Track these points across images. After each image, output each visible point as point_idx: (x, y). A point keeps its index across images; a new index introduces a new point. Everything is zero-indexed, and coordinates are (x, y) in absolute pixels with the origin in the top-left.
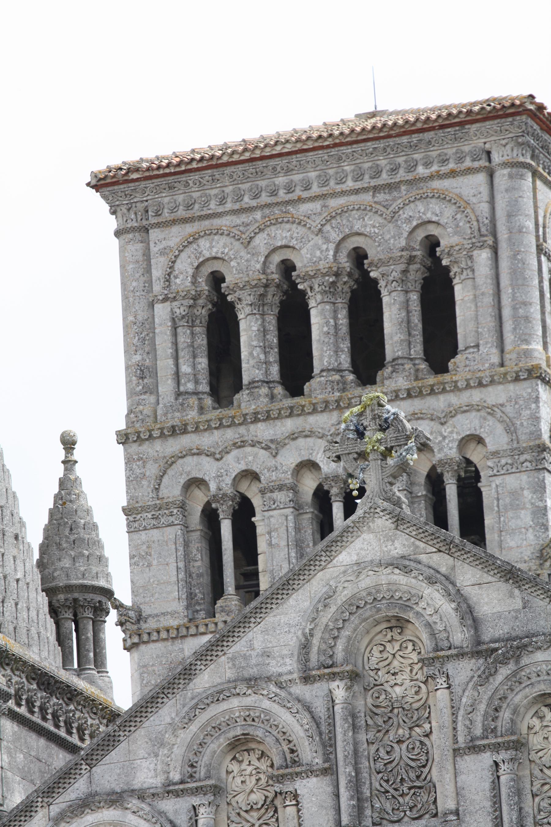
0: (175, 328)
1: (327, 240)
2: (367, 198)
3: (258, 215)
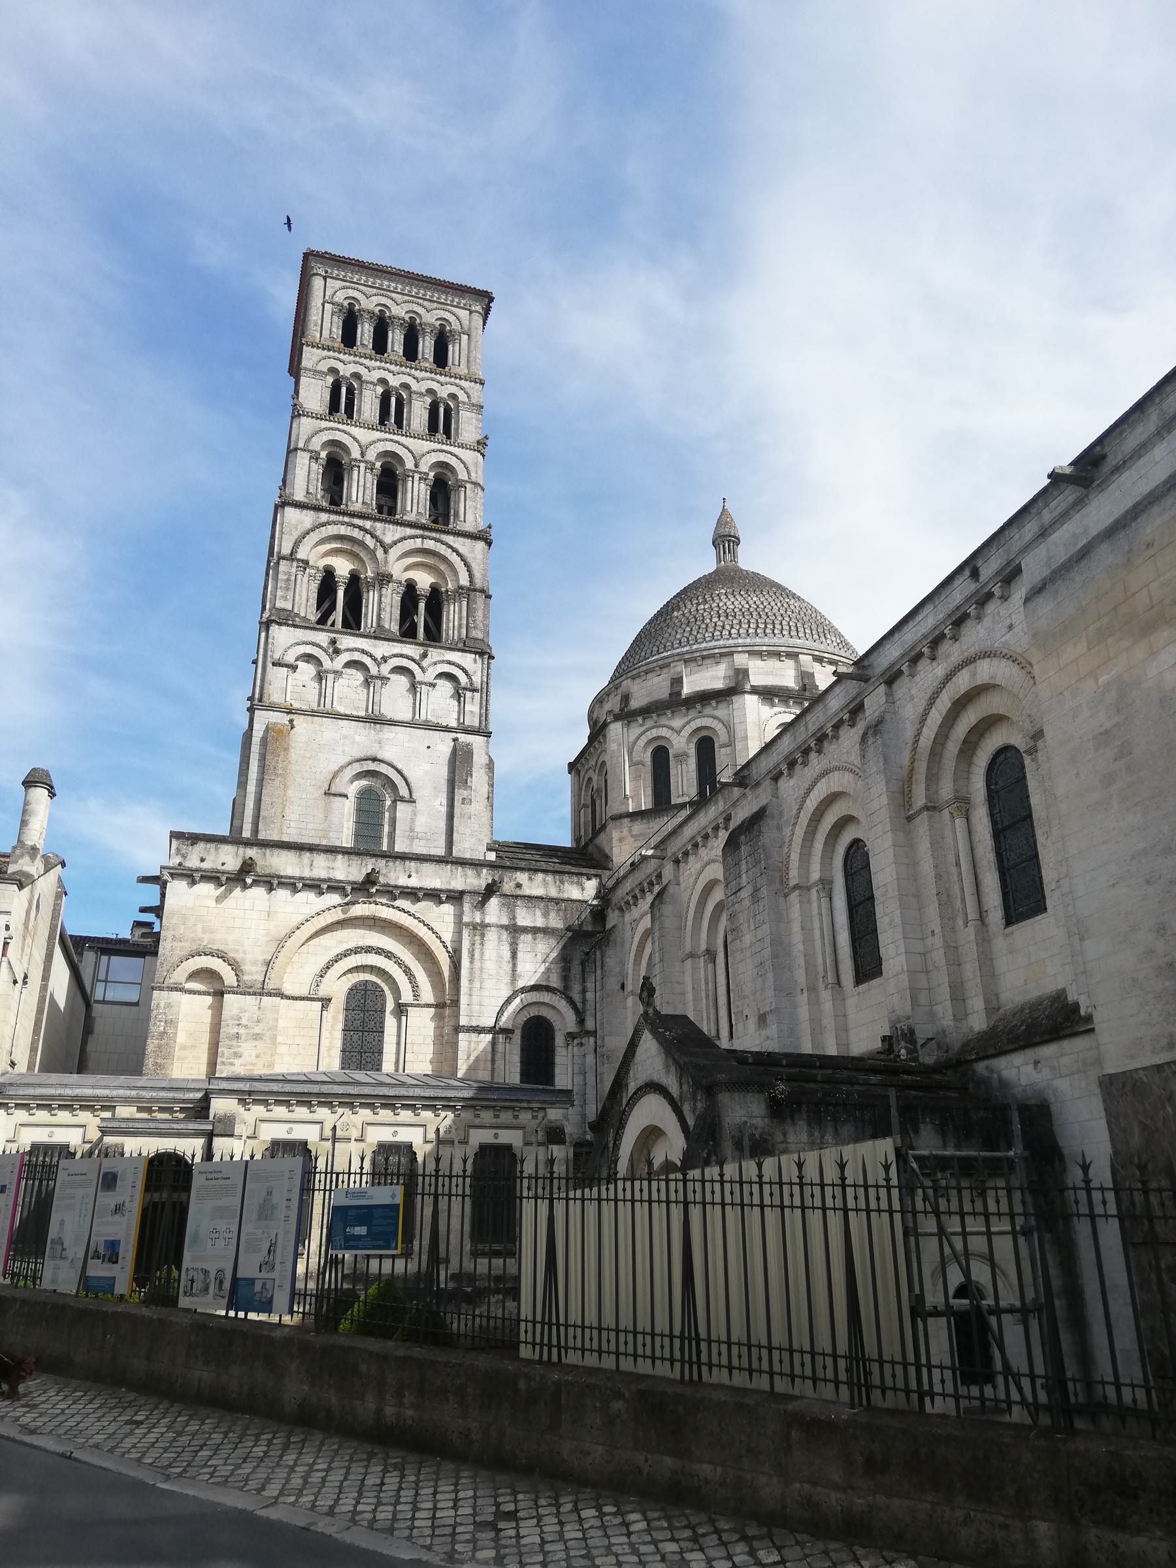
2: (421, 301)
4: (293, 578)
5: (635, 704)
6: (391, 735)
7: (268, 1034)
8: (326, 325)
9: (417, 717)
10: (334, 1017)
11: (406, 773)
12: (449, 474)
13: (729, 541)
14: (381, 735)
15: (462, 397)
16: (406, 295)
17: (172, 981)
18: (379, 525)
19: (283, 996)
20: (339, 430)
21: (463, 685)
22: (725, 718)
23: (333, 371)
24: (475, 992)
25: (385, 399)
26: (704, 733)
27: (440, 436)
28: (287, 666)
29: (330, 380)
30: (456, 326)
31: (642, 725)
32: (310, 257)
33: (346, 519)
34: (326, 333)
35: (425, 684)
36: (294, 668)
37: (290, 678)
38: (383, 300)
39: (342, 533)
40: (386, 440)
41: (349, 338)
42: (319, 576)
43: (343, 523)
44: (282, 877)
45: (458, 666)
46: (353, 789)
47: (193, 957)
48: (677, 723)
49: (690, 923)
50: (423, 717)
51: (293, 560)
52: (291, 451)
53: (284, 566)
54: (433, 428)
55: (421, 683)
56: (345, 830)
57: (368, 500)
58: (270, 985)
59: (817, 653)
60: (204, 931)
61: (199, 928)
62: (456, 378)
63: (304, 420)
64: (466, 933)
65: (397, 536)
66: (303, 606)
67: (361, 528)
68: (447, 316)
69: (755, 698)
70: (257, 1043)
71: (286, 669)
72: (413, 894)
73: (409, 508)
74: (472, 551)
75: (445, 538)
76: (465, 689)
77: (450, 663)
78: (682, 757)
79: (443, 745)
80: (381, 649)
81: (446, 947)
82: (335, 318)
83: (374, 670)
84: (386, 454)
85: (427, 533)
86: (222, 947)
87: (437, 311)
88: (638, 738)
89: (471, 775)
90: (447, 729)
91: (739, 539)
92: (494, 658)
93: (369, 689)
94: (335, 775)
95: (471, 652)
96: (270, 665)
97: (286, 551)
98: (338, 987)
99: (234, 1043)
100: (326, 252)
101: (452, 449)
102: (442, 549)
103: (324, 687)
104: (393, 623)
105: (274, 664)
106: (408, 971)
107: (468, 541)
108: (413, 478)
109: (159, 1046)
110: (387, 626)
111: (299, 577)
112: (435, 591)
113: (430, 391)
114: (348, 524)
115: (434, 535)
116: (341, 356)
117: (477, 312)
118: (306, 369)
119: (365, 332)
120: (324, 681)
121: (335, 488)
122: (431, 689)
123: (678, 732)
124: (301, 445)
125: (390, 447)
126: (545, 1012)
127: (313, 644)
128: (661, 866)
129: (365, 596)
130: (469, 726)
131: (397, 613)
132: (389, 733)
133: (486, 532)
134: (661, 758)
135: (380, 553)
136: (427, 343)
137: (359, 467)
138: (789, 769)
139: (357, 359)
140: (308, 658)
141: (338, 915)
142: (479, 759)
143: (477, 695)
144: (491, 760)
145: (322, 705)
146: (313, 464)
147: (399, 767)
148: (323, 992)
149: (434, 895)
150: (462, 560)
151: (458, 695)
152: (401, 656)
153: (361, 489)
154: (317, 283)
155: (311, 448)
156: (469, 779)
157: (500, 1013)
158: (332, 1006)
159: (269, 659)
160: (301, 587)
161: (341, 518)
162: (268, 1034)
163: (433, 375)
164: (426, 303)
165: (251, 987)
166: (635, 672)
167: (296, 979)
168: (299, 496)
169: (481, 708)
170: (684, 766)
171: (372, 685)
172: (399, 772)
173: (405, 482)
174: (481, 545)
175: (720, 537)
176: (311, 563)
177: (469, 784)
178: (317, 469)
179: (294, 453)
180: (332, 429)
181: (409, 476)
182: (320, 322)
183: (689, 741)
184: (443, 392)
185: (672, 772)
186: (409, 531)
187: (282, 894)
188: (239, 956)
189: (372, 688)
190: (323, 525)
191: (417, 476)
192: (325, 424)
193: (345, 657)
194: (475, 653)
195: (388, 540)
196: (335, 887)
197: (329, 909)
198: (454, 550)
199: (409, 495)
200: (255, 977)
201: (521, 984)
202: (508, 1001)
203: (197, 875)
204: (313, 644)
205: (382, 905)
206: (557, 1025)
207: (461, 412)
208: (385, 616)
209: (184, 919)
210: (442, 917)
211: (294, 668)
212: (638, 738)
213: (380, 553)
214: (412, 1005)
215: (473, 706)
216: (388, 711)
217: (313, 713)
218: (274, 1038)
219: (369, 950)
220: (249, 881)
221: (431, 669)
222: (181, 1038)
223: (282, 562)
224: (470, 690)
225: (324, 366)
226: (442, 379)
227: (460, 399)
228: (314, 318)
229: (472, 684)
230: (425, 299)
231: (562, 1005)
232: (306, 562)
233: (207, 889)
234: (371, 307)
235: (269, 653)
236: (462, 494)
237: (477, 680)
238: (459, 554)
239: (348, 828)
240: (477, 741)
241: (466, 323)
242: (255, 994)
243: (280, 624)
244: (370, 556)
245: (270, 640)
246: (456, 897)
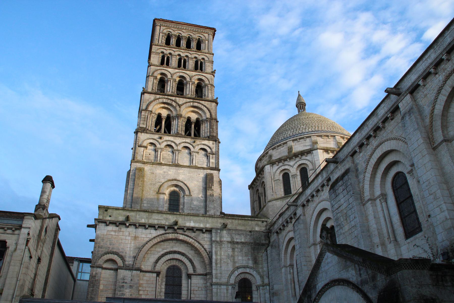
0: (162, 36)
1: (186, 34)
3: (176, 29)
4: (146, 117)
5: (274, 158)
6: (182, 171)
7: (135, 286)
8: (160, 39)
9: (192, 164)
10: (162, 280)
11: (188, 185)
12: (202, 83)
13: (302, 104)
14: (178, 171)
15: (206, 59)
16: (187, 30)
17: (98, 264)
18: (177, 98)
19: (141, 271)
20: (164, 70)
21: (209, 152)
22: (310, 160)
23: (162, 52)
24: (219, 269)
25: (180, 60)
26: (303, 166)
27: (199, 70)
28: (144, 147)
29: (161, 55)
30: (203, 38)
31: (278, 165)
32: (156, 20)
33: (166, 97)
34: (160, 42)
35: (195, 152)
36: (146, 147)
37: (145, 151)
38: (179, 32)
39: (164, 101)
40: (180, 72)
41: (168, 42)
42: (156, 116)
43: (164, 98)
44: (140, 223)
45: (207, 146)
46: (167, 192)
47: (106, 254)
48: (292, 163)
49: (311, 230)
50: (194, 164)
51: (146, 111)
52: (148, 77)
53: (143, 113)
54: (196, 68)
55: (193, 152)
56: (165, 207)
57: (173, 91)
58: (137, 266)
59: (342, 136)
60: (110, 245)
61: (108, 243)
62: (204, 53)
63: (152, 67)
64: (214, 245)
65: (184, 102)
66: (150, 127)
67: (171, 100)
68: (201, 35)
69: (322, 151)
70: (130, 289)
71: (143, 148)
72: (191, 229)
73: (188, 93)
74: (211, 106)
75: (201, 102)
76: (209, 154)
77: (204, 145)
78: (294, 176)
79: (202, 174)
80: (178, 140)
81: (206, 250)
82: (163, 38)
83: (175, 148)
84: (181, 77)
85: (195, 101)
86: (117, 251)
87: (197, 35)
88: (277, 170)
89: (213, 185)
90: (204, 168)
91: (305, 104)
92: (220, 143)
93: (174, 155)
94: (160, 186)
95: (211, 140)
96: (137, 146)
97: (144, 108)
98: (162, 267)
99: (122, 289)
100: (161, 19)
101: (203, 74)
102: (200, 106)
103: (157, 154)
104: (182, 132)
105: (139, 146)
106: (191, 261)
107: (209, 103)
108: (189, 84)
109: (93, 290)
110: (180, 132)
111: (149, 116)
112: (198, 120)
113: (196, 58)
114: (166, 98)
115: (197, 101)
116: (165, 48)
117: (211, 34)
118: (153, 52)
119: (173, 41)
120: (157, 152)
121: (162, 89)
122: (197, 154)
123: (292, 167)
124: (151, 75)
125: (181, 74)
126: (247, 276)
127: (153, 139)
128: (296, 210)
129: (172, 123)
130: (211, 167)
131: (184, 128)
132: (181, 170)
133: (216, 100)
134: (286, 177)
135: (178, 108)
136: (194, 44)
137: (170, 81)
138: (359, 149)
139: (170, 49)
140: (152, 144)
141: (163, 238)
142: (215, 179)
143: (214, 156)
144: (220, 180)
145: (156, 161)
146: (155, 81)
147: (185, 183)
148: (158, 268)
149: (201, 230)
150: (207, 109)
151: (207, 156)
152: (186, 142)
153: (171, 88)
154: (158, 28)
155: (154, 75)
156: (212, 187)
157: (230, 276)
158: (161, 276)
159: (137, 145)
160: (149, 120)
161: (164, 97)
162: (135, 286)
163: (196, 53)
164: (193, 32)
165: (128, 267)
166: (273, 147)
167: (147, 265)
168: (150, 90)
169: (216, 161)
170: (296, 179)
171: (174, 153)
172: (186, 185)
173: (186, 85)
174: (214, 104)
175: (299, 103)
176: (153, 112)
177: (212, 188)
178: (156, 82)
179: (148, 78)
180: (162, 69)
181: (188, 83)
182: (158, 38)
183: (297, 170)
184: (200, 57)
185: (291, 182)
186: (188, 100)
187: (140, 230)
188: (123, 254)
189: (175, 154)
190: (158, 99)
191: (191, 83)
192: (159, 68)
193: (165, 143)
194: (213, 141)
195: (180, 103)
196: (161, 227)
197: (159, 236)
198: (204, 106)
199: (188, 89)
200: (130, 263)
201: (237, 265)
202: (233, 272)
203: (108, 223)
204: (153, 139)
206: (253, 281)
207: (206, 63)
208: (180, 129)
209: (103, 240)
210: (205, 239)
211: (146, 147)
212: (277, 170)
213: (178, 108)
214: (193, 275)
215: (212, 160)
216: (181, 163)
217: (153, 164)
218: (138, 288)
219: (175, 252)
220: (127, 224)
221: (197, 147)
222: (101, 287)
223: (143, 112)
224: (212, 154)
225: (159, 51)
226: (199, 53)
227: (206, 59)
228: (157, 38)
229: (212, 152)
230: (193, 31)
231: (254, 273)
232: (151, 111)
233: (111, 228)
234: (175, 34)
235: (137, 143)
236: (207, 88)
237: (214, 150)
238: (206, 107)
239: (166, 207)
240: (215, 172)
241: (207, 37)
242: (130, 270)
243: (141, 132)
244: (174, 109)
245: (138, 138)
246: (209, 231)
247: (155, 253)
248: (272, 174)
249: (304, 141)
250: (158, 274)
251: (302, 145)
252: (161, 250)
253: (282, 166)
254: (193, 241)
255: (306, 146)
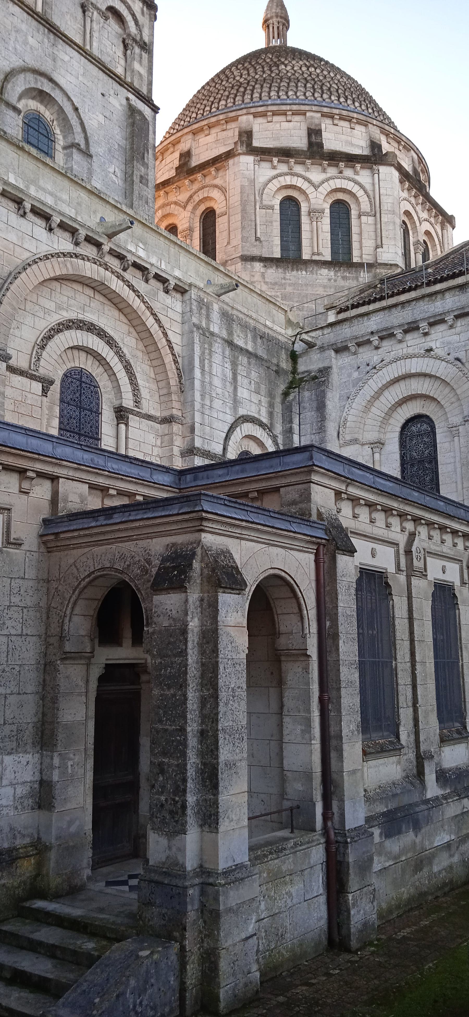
22: (368, 187)
31: (274, 168)
106: (128, 368)
123: (316, 187)
205: (113, 273)
247: (38, 314)
248: (257, 188)
249: (349, 130)
250: (46, 383)
251: (344, 137)
252: (50, 305)
253: (286, 174)
254: (143, 307)
255: (352, 145)
